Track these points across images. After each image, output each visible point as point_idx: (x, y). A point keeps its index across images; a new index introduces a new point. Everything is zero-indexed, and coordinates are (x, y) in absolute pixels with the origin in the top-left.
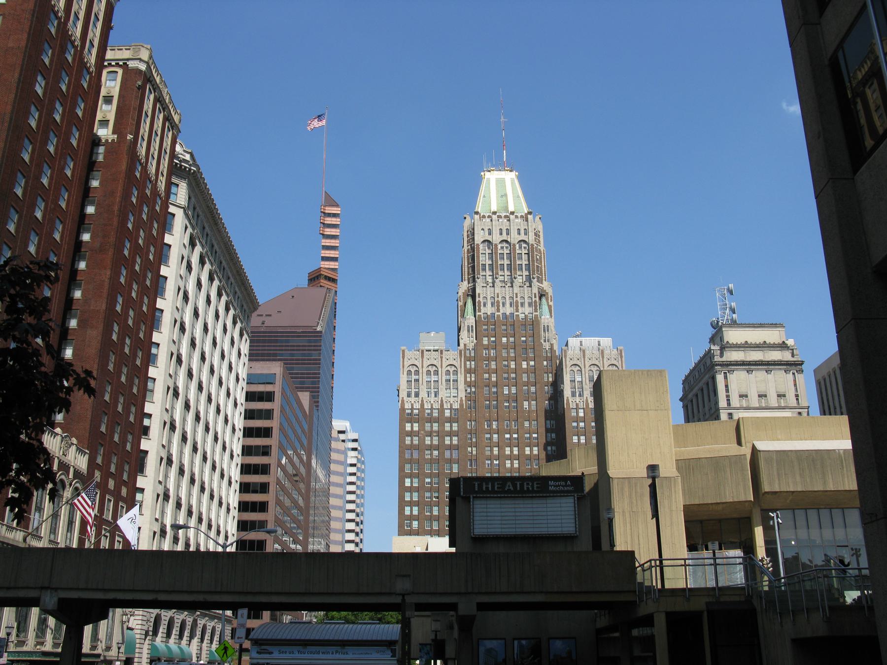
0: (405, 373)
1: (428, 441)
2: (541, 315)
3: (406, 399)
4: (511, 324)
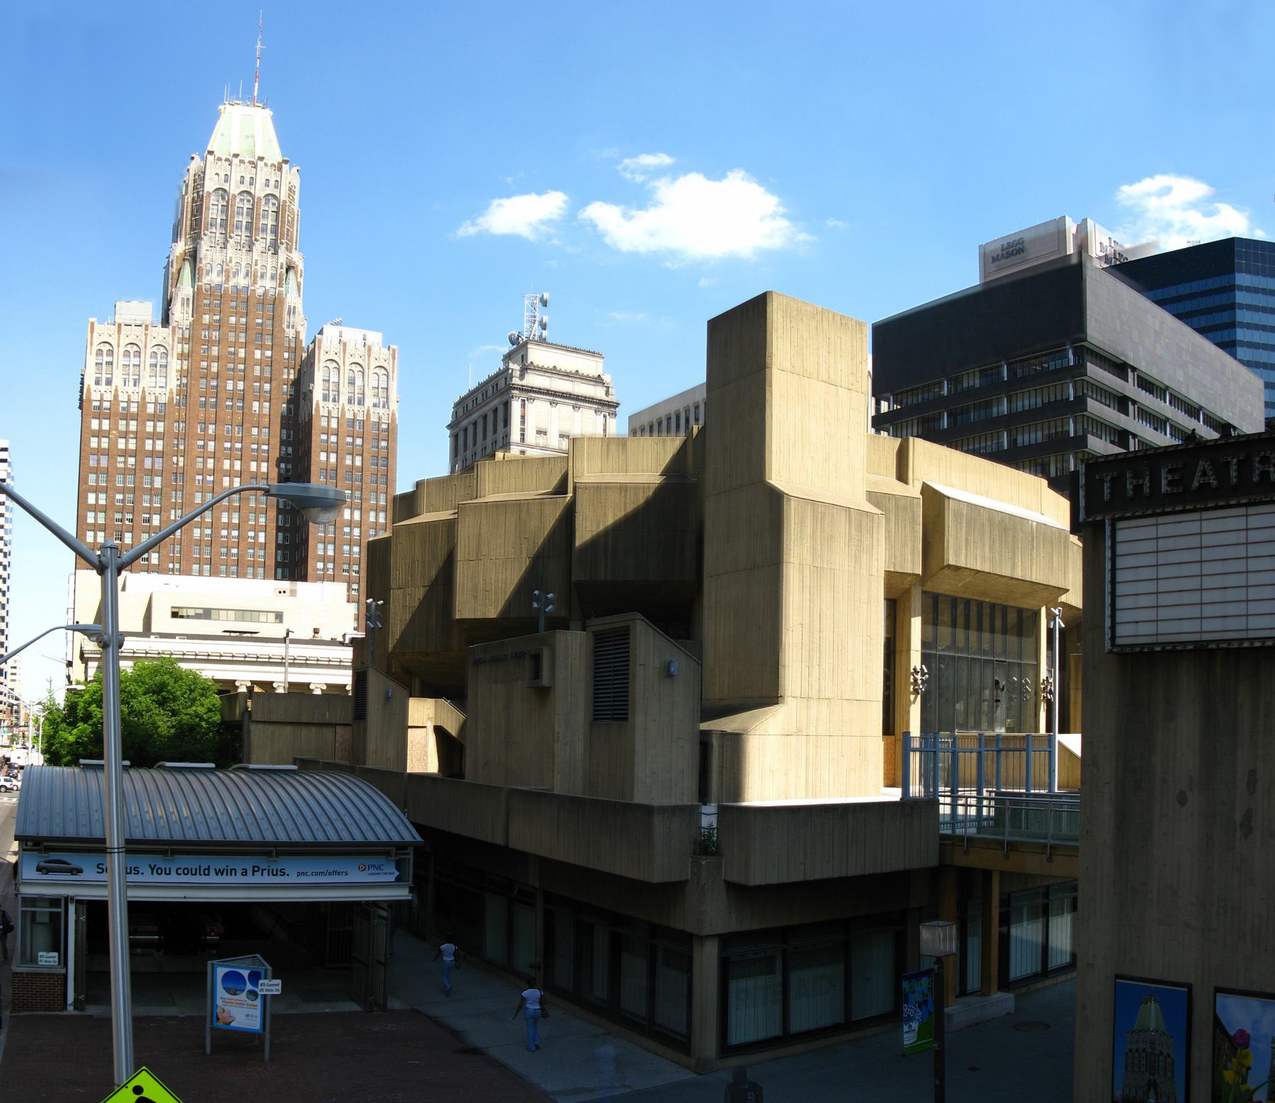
0: (94, 352)
1: (121, 444)
2: (287, 292)
3: (93, 387)
4: (245, 301)
